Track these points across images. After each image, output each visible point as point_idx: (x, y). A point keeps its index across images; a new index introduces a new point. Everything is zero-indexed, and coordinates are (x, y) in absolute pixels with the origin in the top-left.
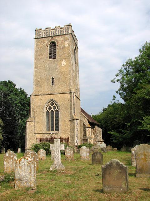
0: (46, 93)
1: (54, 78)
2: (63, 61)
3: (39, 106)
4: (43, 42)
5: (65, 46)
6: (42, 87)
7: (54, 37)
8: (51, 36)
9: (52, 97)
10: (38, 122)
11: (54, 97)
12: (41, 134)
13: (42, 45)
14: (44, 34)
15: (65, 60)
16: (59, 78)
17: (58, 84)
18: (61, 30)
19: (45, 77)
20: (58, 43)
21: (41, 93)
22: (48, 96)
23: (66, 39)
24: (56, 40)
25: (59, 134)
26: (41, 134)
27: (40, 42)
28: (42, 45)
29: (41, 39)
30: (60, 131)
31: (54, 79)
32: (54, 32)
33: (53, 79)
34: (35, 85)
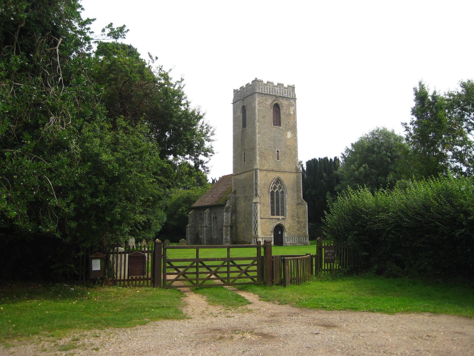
0: (271, 168)
3: (265, 184)
5: (290, 113)
6: (266, 160)
7: (278, 98)
8: (275, 96)
10: (264, 204)
11: (282, 177)
13: (265, 104)
14: (267, 89)
15: (291, 131)
16: (285, 153)
17: (284, 160)
18: (285, 91)
19: (269, 148)
20: (283, 106)
21: (266, 168)
24: (280, 103)
25: (286, 220)
27: (262, 99)
28: (265, 104)
29: (263, 95)
30: (287, 217)
31: (280, 153)
32: (277, 89)
33: (278, 151)
34: (259, 157)
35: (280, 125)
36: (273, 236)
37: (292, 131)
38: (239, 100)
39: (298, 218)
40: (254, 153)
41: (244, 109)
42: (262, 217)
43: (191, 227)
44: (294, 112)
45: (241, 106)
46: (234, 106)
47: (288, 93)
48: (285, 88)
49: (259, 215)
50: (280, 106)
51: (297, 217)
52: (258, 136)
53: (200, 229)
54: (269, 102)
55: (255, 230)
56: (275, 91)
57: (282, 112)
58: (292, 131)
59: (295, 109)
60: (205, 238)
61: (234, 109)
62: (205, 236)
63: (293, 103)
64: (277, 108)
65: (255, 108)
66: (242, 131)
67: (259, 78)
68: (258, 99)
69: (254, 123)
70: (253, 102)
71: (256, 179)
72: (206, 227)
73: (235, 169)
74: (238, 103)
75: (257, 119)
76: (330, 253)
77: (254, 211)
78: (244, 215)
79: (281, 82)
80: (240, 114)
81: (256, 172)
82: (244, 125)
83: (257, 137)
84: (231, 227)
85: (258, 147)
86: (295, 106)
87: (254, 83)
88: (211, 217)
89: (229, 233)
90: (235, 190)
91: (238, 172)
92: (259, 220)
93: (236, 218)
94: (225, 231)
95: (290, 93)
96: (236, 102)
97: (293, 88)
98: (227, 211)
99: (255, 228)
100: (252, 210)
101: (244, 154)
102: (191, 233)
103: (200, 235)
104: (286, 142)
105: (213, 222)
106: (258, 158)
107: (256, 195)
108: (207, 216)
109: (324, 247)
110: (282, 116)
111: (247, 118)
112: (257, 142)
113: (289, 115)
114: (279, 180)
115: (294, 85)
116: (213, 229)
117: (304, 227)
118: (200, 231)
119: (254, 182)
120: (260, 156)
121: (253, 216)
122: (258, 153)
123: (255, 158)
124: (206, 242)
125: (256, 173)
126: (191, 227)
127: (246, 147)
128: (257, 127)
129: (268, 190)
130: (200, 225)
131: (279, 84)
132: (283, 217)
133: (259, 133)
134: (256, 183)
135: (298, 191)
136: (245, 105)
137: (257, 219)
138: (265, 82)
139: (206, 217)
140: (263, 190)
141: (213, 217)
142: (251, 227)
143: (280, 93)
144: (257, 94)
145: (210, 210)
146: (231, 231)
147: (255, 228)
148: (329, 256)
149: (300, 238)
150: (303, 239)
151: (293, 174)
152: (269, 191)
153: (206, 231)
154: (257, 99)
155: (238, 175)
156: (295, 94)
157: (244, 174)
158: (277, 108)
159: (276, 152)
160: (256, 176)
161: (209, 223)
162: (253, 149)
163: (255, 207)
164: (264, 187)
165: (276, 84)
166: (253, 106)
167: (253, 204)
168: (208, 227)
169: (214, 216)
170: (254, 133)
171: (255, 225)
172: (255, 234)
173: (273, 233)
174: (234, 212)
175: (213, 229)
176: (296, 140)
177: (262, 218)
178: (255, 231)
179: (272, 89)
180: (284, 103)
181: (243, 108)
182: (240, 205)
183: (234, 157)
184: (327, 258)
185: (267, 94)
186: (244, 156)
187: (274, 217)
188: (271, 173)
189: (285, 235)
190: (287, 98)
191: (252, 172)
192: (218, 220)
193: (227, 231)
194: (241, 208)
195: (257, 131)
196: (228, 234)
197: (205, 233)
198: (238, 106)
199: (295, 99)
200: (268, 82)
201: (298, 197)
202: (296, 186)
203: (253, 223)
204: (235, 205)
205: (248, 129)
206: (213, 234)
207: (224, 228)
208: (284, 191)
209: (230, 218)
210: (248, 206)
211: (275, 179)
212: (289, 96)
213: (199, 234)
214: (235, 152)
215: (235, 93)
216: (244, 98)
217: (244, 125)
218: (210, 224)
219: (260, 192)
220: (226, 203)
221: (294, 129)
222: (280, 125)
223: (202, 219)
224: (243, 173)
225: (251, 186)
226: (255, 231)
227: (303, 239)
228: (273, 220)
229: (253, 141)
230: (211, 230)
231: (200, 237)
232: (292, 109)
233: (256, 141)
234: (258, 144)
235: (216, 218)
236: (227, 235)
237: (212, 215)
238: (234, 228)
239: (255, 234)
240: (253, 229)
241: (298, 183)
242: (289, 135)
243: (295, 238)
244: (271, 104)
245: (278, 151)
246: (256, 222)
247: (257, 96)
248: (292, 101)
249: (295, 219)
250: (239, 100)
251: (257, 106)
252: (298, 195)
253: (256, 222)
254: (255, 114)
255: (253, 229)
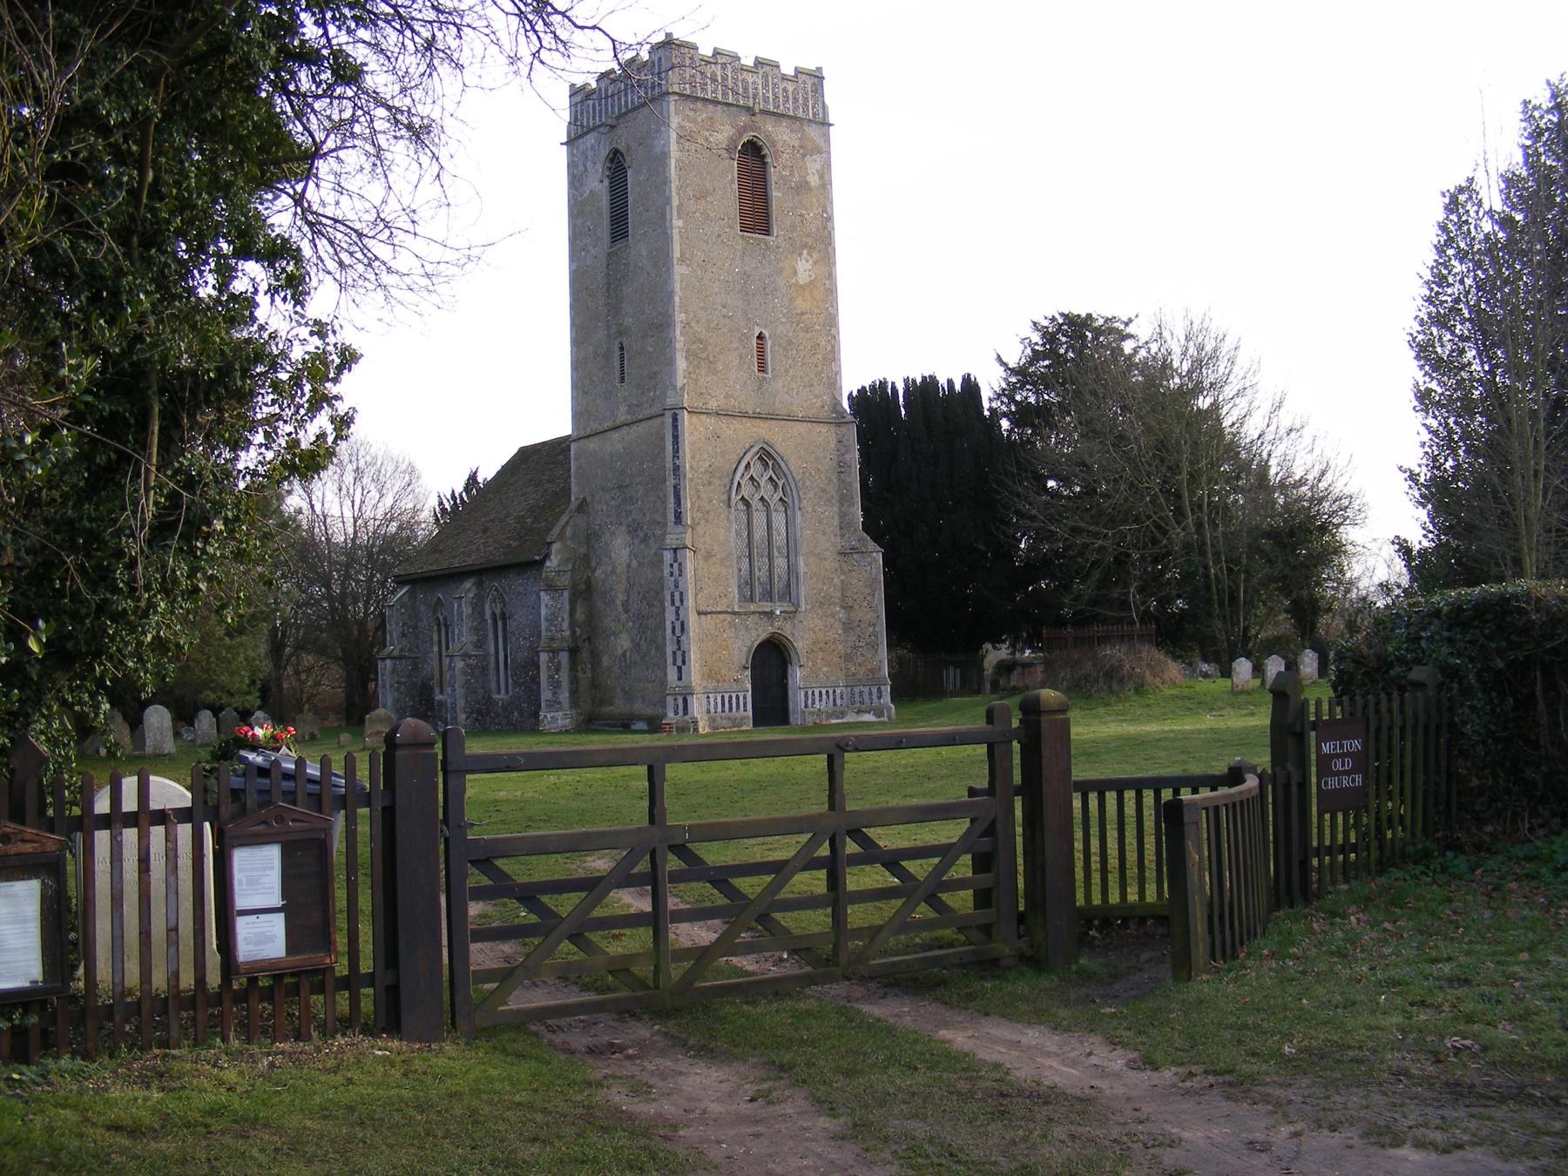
1: (766, 333)
2: (800, 255)
3: (711, 472)
4: (711, 124)
5: (807, 183)
6: (715, 372)
9: (762, 430)
10: (709, 556)
11: (780, 437)
12: (727, 612)
16: (790, 342)
17: (787, 371)
18: (785, 90)
19: (727, 321)
21: (713, 404)
22: (748, 423)
23: (809, 146)
24: (767, 137)
26: (727, 612)
27: (694, 121)
29: (699, 105)
31: (769, 343)
33: (760, 337)
35: (768, 232)
36: (749, 686)
37: (816, 256)
38: (594, 129)
39: (848, 608)
40: (669, 343)
41: (617, 166)
42: (702, 608)
43: (400, 658)
44: (821, 177)
45: (604, 152)
46: (571, 155)
47: (796, 100)
48: (784, 78)
49: (690, 601)
50: (765, 151)
51: (842, 607)
52: (679, 270)
53: (435, 663)
54: (723, 133)
55: (679, 663)
56: (746, 89)
57: (773, 175)
58: (816, 256)
59: (828, 164)
60: (461, 703)
61: (572, 166)
62: (460, 692)
63: (820, 142)
64: (753, 154)
65: (665, 156)
66: (609, 255)
67: (680, 34)
68: (677, 117)
69: (662, 218)
70: (658, 131)
71: (676, 451)
72: (466, 656)
73: (578, 415)
74: (590, 139)
75: (675, 202)
76: (1343, 756)
77: (672, 585)
78: (625, 604)
79: (766, 54)
80: (598, 184)
81: (675, 419)
82: (619, 226)
83: (677, 277)
84: (574, 652)
85: (679, 317)
86: (823, 150)
87: (660, 53)
88: (482, 614)
89: (564, 677)
90: (585, 499)
91: (595, 426)
92: (693, 620)
93: (592, 616)
94: (549, 668)
95: (806, 99)
96: (581, 136)
97: (817, 77)
98: (551, 588)
99: (679, 654)
100: (661, 580)
101: (622, 349)
102: (398, 682)
103: (437, 690)
104: (792, 300)
105: (491, 635)
106: (681, 364)
107: (678, 518)
108: (467, 610)
109: (1314, 726)
110: (776, 194)
111: (630, 199)
112: (677, 299)
113: (803, 187)
114: (770, 455)
115: (819, 69)
116: (492, 666)
117: (874, 646)
118: (437, 673)
119: (669, 465)
120: (689, 355)
121: (667, 604)
122: (680, 341)
123: (671, 362)
124: (464, 716)
125: (675, 427)
126: (400, 658)
127: (629, 321)
128: (676, 237)
129: (725, 497)
130: (436, 649)
131: (759, 62)
132: (787, 606)
133: (682, 260)
134: (676, 469)
135: (844, 499)
136: (622, 148)
137: (687, 615)
138: (706, 50)
139: (460, 613)
140: (703, 495)
141: (494, 614)
142: (661, 650)
143: (766, 100)
144: (672, 98)
145: (479, 585)
146: (571, 669)
147: (679, 654)
148: (1339, 773)
149: (857, 690)
150: (870, 694)
151: (823, 429)
152: (729, 499)
153: (466, 673)
154: (675, 121)
155: (595, 439)
156: (824, 106)
157: (624, 430)
158: (753, 154)
159: (755, 341)
160: (676, 438)
161: (475, 638)
162: (661, 327)
163: (676, 565)
164: (710, 484)
165: (748, 61)
166: (658, 150)
167: (668, 556)
168: (470, 657)
169: (498, 611)
170: (662, 258)
171: (679, 642)
172: (680, 678)
173: (748, 672)
174: (584, 591)
175: (492, 666)
176: (831, 291)
177: (706, 613)
178: (680, 669)
179: (735, 80)
180: (779, 136)
181: (612, 160)
182: (605, 559)
183: (577, 365)
184: (1332, 783)
185: (715, 102)
186: (622, 358)
187: (752, 607)
188: (736, 424)
189: (797, 676)
190: (795, 118)
191: (656, 422)
192: (512, 625)
193: (557, 670)
194: (613, 572)
195: (677, 254)
196: (558, 682)
197: (460, 679)
198: (590, 154)
199: (826, 124)
200: (717, 53)
201: (845, 526)
202: (834, 477)
203: (669, 631)
204: (584, 563)
205: (638, 246)
206: (493, 685)
207: (544, 657)
208: (790, 503)
209: (566, 616)
210: (640, 564)
211: (755, 450)
212: (800, 114)
213: (432, 688)
214: (578, 342)
215: (578, 98)
216: (617, 118)
217: (619, 226)
218: (480, 644)
219: (692, 504)
220: (547, 556)
221: (822, 243)
222: (768, 232)
223: (445, 626)
224: (616, 428)
225: (657, 481)
226: (680, 669)
227: (870, 694)
228: (750, 620)
229: (660, 294)
230: (485, 669)
231: (438, 697)
232: (813, 165)
233: (671, 295)
234: (682, 305)
235: (504, 617)
236: (556, 685)
237: (487, 607)
238: (584, 655)
239: (680, 678)
240: (670, 660)
241: (842, 467)
242: (804, 268)
243: (838, 691)
244: (733, 141)
245: (760, 337)
246: (683, 630)
247: (672, 108)
248: (813, 132)
249: (833, 615)
250: (594, 129)
251: (673, 147)
252: (842, 515)
253: (683, 630)
254: (666, 182)
255: (670, 660)
